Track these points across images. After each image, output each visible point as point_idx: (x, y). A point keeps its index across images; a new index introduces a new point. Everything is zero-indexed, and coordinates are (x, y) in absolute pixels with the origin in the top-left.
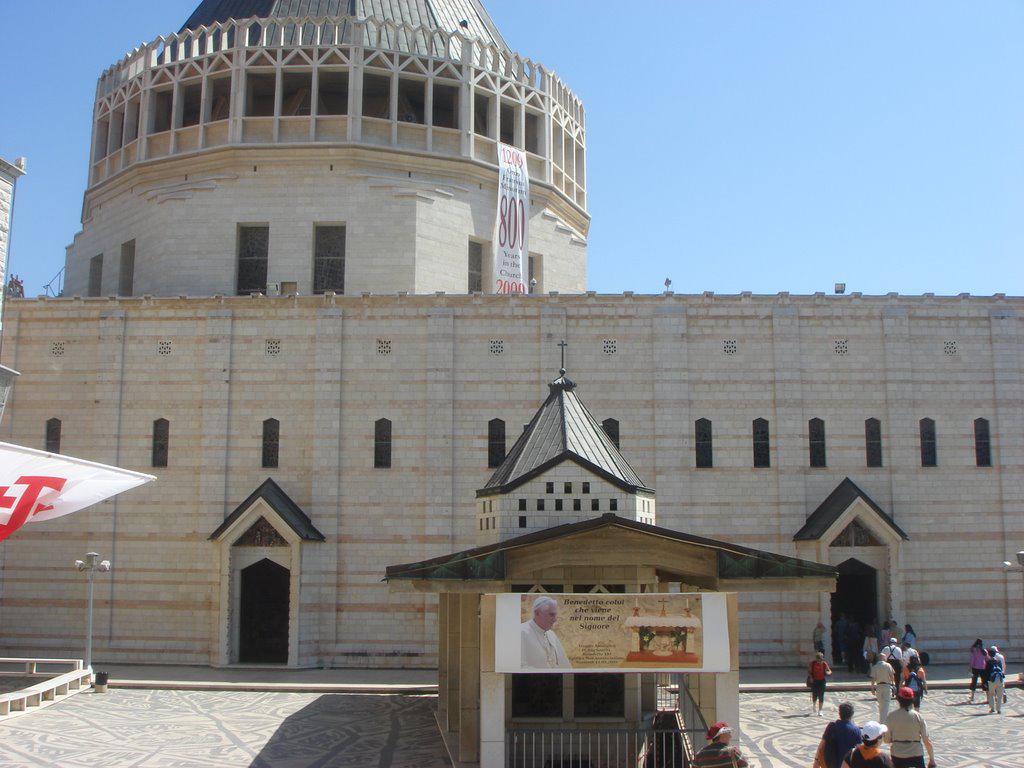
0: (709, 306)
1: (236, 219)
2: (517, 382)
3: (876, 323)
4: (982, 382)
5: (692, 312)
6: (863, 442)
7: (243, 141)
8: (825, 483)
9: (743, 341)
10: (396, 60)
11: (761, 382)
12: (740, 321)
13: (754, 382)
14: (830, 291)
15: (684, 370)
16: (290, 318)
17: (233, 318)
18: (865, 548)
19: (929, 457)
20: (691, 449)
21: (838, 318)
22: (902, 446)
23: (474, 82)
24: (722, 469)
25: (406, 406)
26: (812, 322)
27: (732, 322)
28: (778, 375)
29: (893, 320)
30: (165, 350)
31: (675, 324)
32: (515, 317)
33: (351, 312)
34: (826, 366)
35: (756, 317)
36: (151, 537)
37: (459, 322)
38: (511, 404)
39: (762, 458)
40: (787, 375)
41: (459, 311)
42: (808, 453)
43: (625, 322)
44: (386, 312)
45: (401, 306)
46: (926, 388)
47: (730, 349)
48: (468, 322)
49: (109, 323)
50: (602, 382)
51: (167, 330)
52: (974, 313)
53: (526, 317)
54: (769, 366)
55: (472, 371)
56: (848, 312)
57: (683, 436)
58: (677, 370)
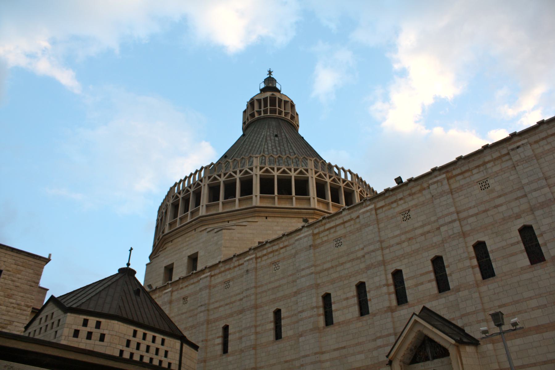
0: (325, 224)
1: (164, 265)
2: (234, 302)
3: (425, 192)
4: (516, 199)
5: (316, 231)
6: (432, 276)
9: (345, 236)
10: (222, 175)
11: (358, 258)
12: (342, 226)
13: (353, 260)
14: (395, 184)
15: (312, 266)
18: (443, 359)
20: (319, 315)
21: (401, 199)
23: (259, 173)
24: (339, 324)
25: (190, 329)
26: (384, 209)
27: (338, 228)
28: (366, 250)
29: (436, 184)
32: (235, 267)
34: (398, 232)
35: (352, 219)
37: (213, 278)
38: (231, 315)
40: (372, 248)
41: (213, 273)
42: (393, 296)
43: (282, 251)
45: (192, 278)
46: (470, 220)
48: (216, 277)
50: (273, 288)
54: (361, 246)
55: (217, 302)
57: (314, 308)
58: (308, 268)
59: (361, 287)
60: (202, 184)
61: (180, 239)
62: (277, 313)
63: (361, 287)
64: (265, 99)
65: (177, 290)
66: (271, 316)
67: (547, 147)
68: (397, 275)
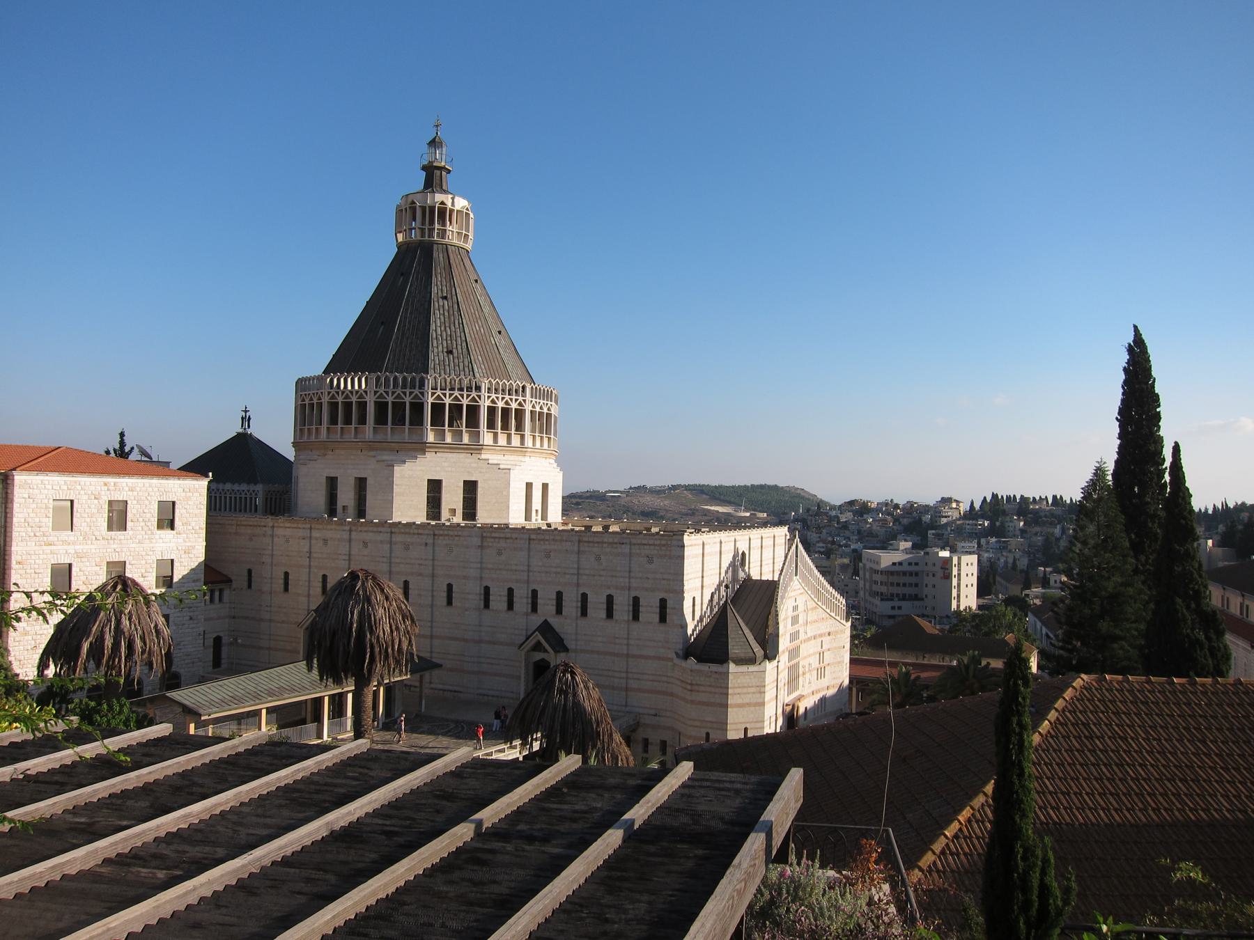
5: (485, 534)
7: (328, 438)
8: (536, 620)
10: (390, 394)
16: (331, 530)
17: (311, 529)
19: (584, 612)
22: (571, 606)
24: (493, 610)
30: (287, 541)
31: (476, 541)
33: (353, 528)
34: (540, 564)
35: (512, 538)
36: (283, 622)
39: (510, 606)
43: (457, 538)
44: (366, 529)
47: (499, 553)
49: (267, 529)
51: (288, 532)
52: (611, 540)
53: (418, 534)
56: (552, 537)
57: (476, 594)
59: (511, 591)
60: (367, 399)
61: (342, 452)
62: (450, 587)
63: (511, 591)
64: (432, 209)
65: (356, 531)
66: (445, 588)
67: (638, 551)
68: (535, 593)
